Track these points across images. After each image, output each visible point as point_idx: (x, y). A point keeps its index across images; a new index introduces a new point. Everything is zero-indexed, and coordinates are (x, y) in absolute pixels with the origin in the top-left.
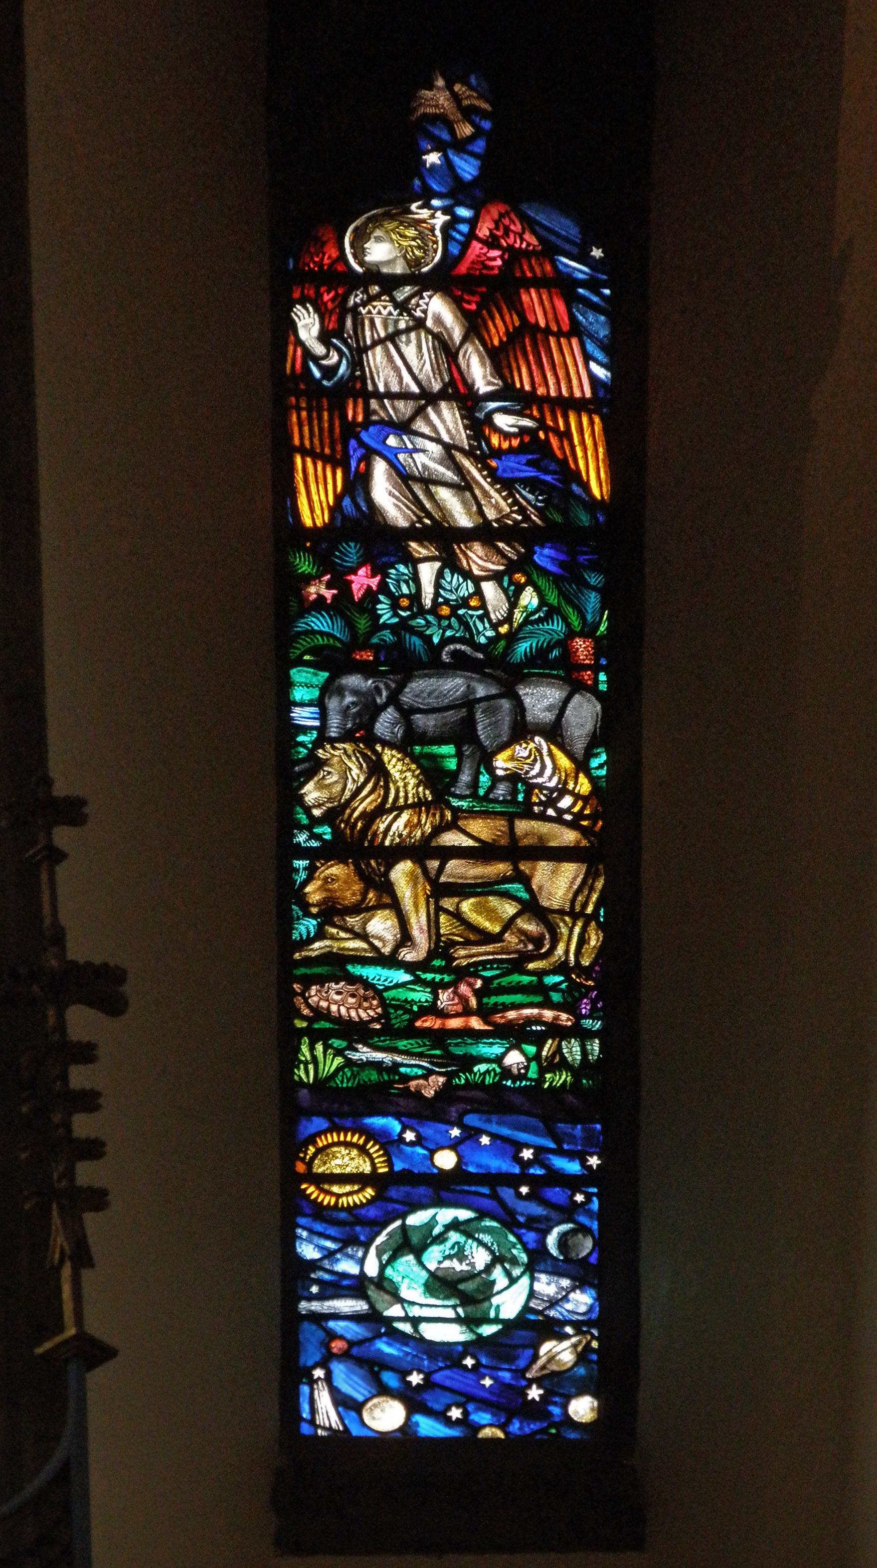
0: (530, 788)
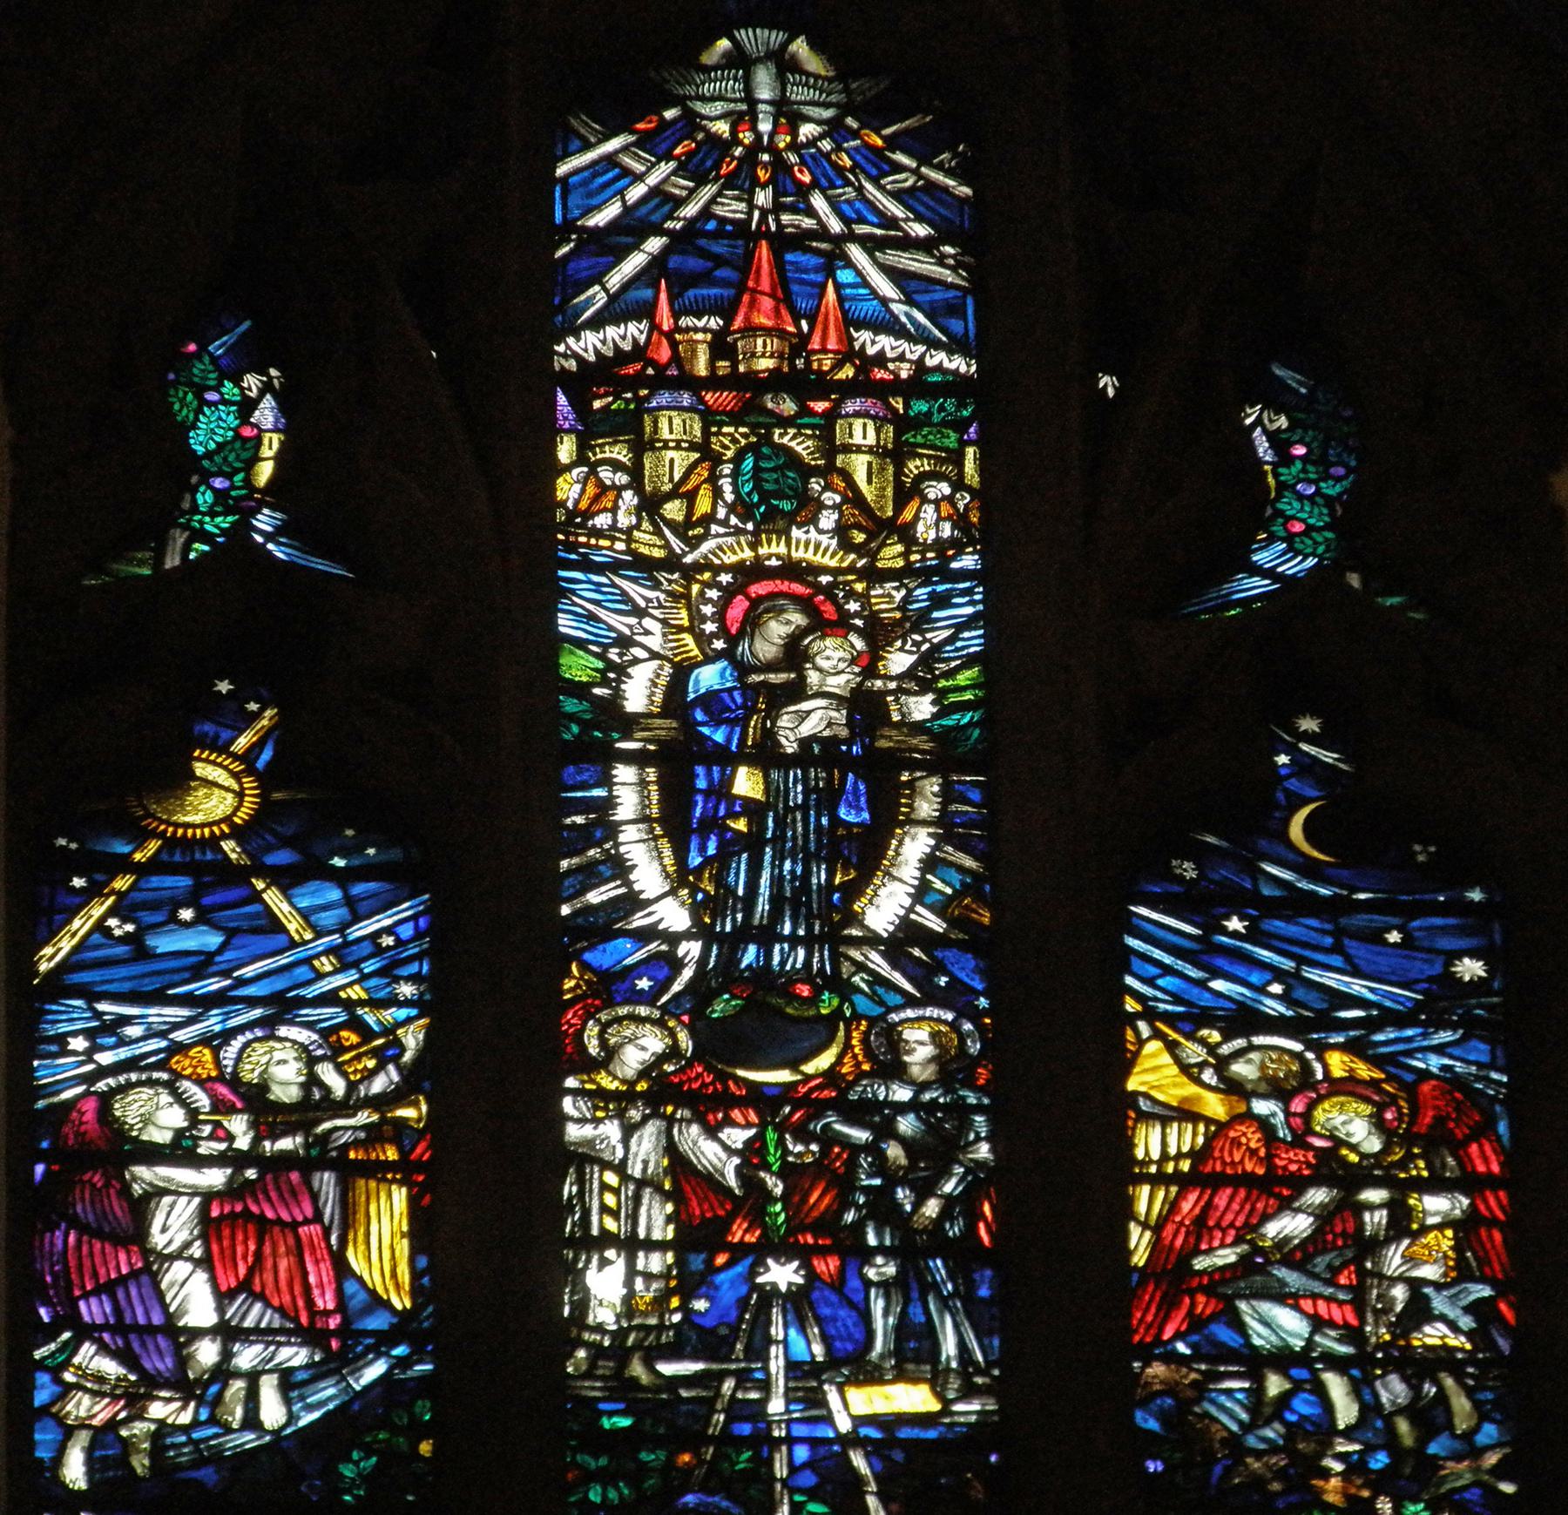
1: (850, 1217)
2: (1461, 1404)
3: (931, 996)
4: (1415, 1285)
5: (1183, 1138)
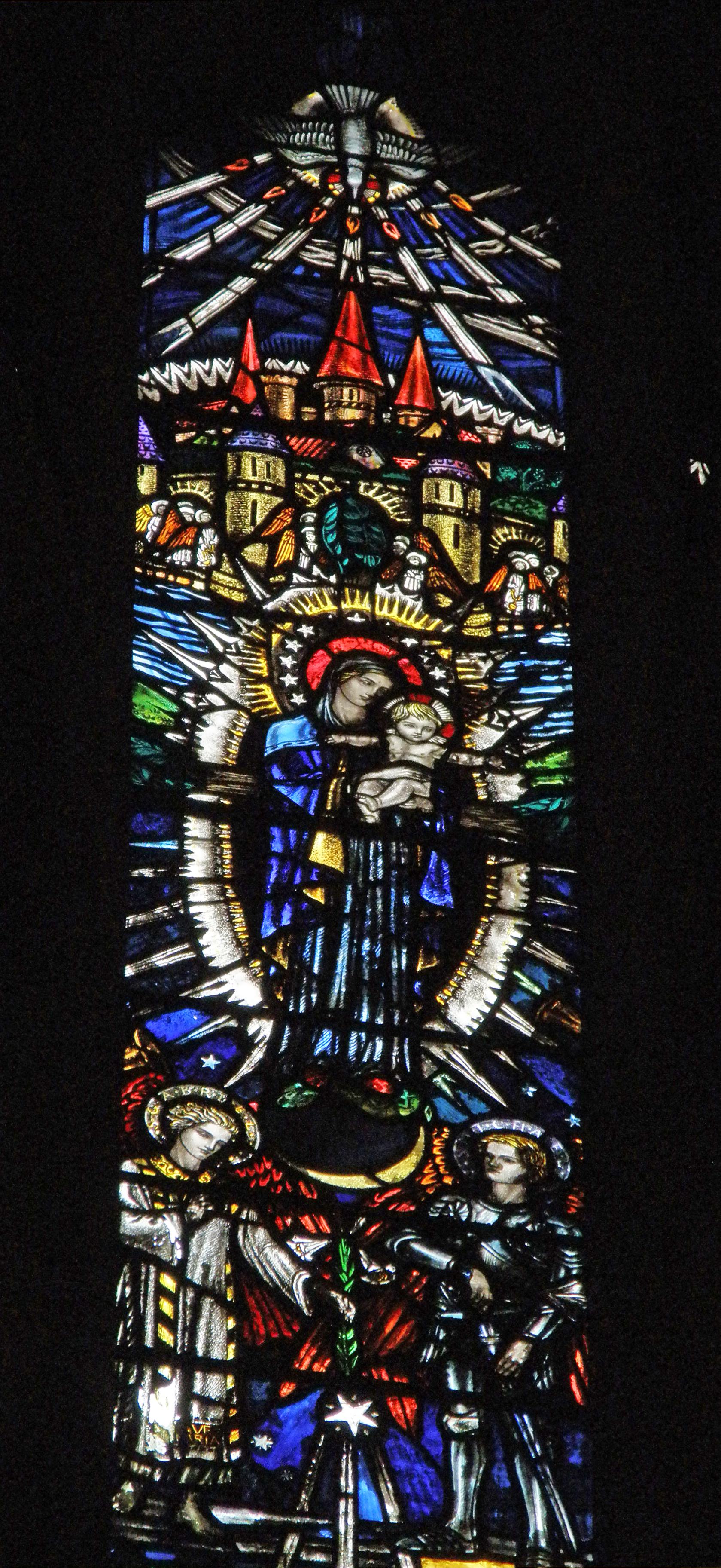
1: (429, 1353)
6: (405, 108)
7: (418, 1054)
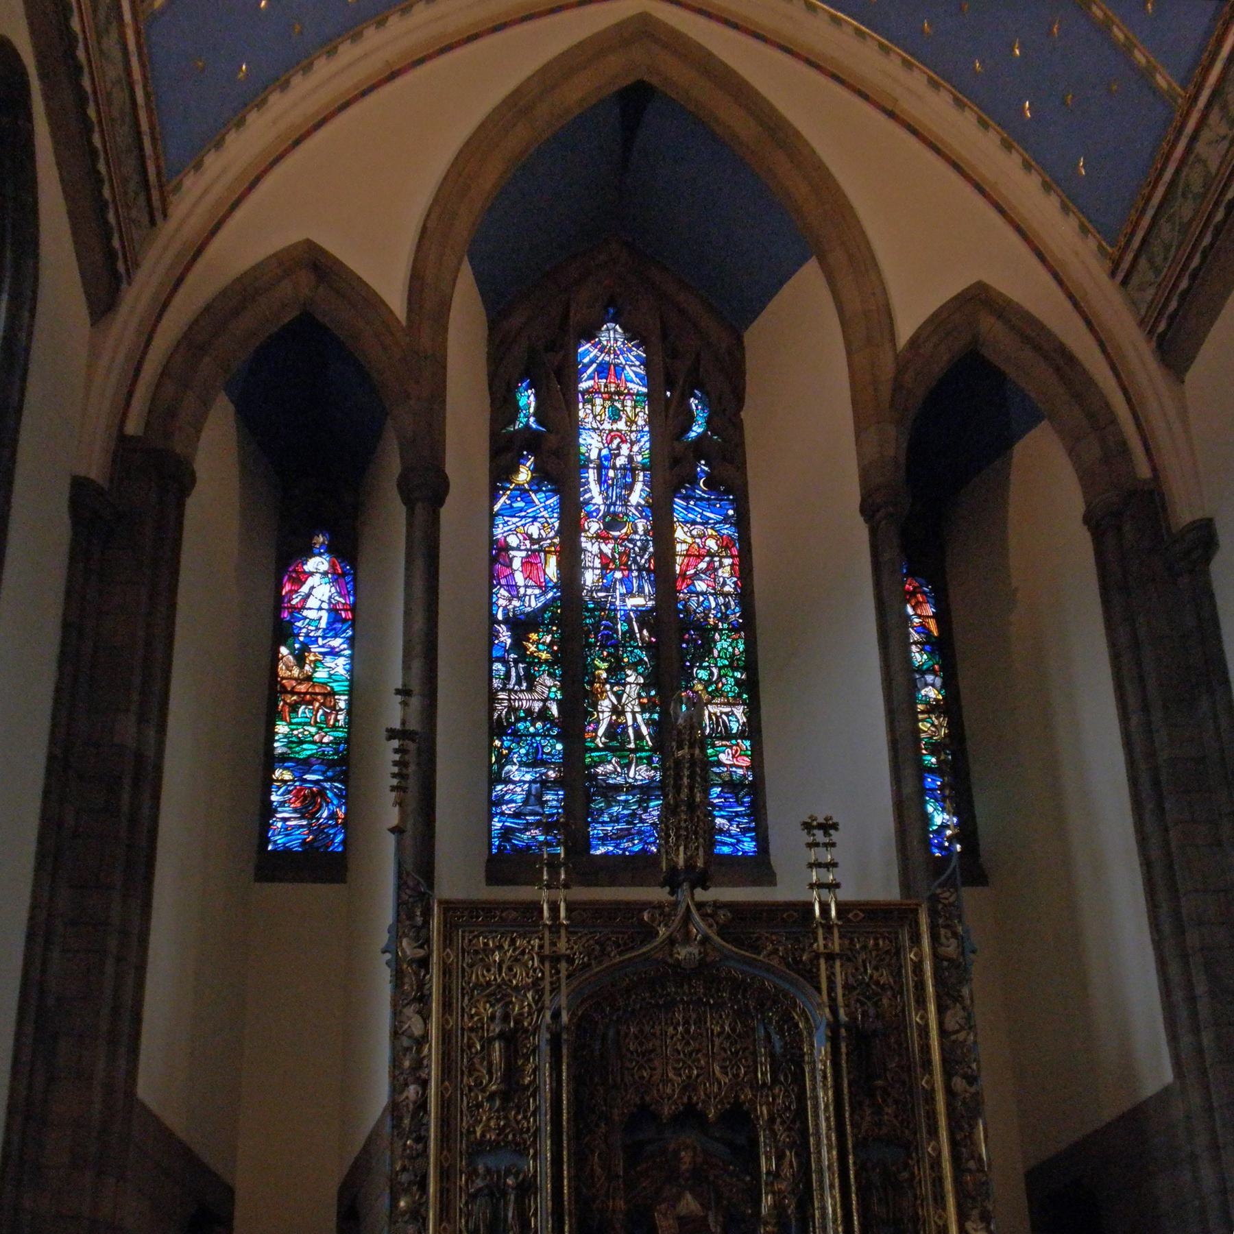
0: (930, 698)
1: (629, 563)
2: (732, 603)
3: (642, 517)
4: (724, 578)
5: (685, 547)
6: (620, 327)
7: (626, 509)
